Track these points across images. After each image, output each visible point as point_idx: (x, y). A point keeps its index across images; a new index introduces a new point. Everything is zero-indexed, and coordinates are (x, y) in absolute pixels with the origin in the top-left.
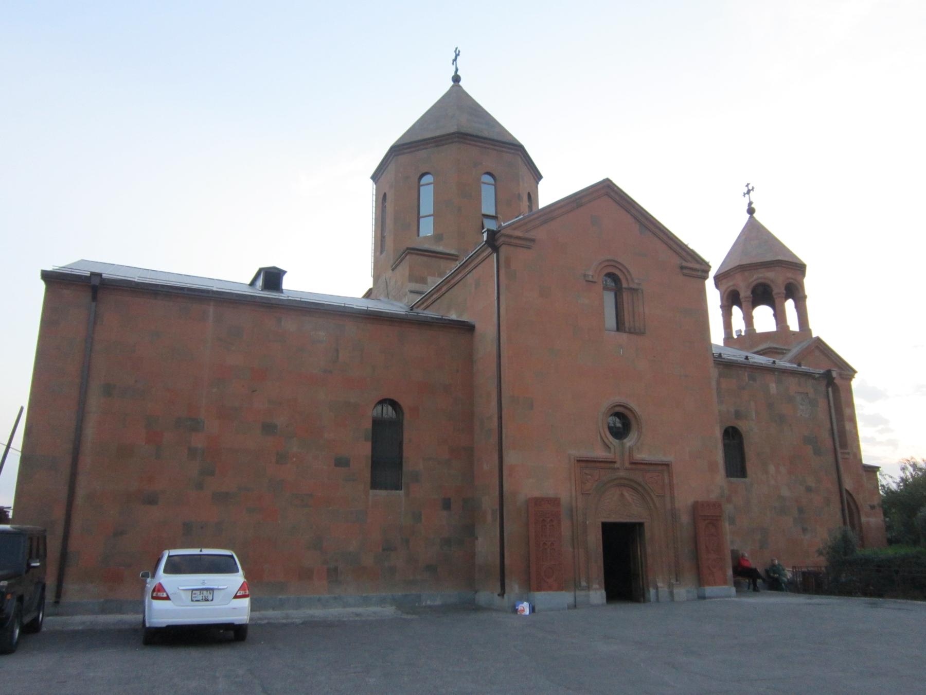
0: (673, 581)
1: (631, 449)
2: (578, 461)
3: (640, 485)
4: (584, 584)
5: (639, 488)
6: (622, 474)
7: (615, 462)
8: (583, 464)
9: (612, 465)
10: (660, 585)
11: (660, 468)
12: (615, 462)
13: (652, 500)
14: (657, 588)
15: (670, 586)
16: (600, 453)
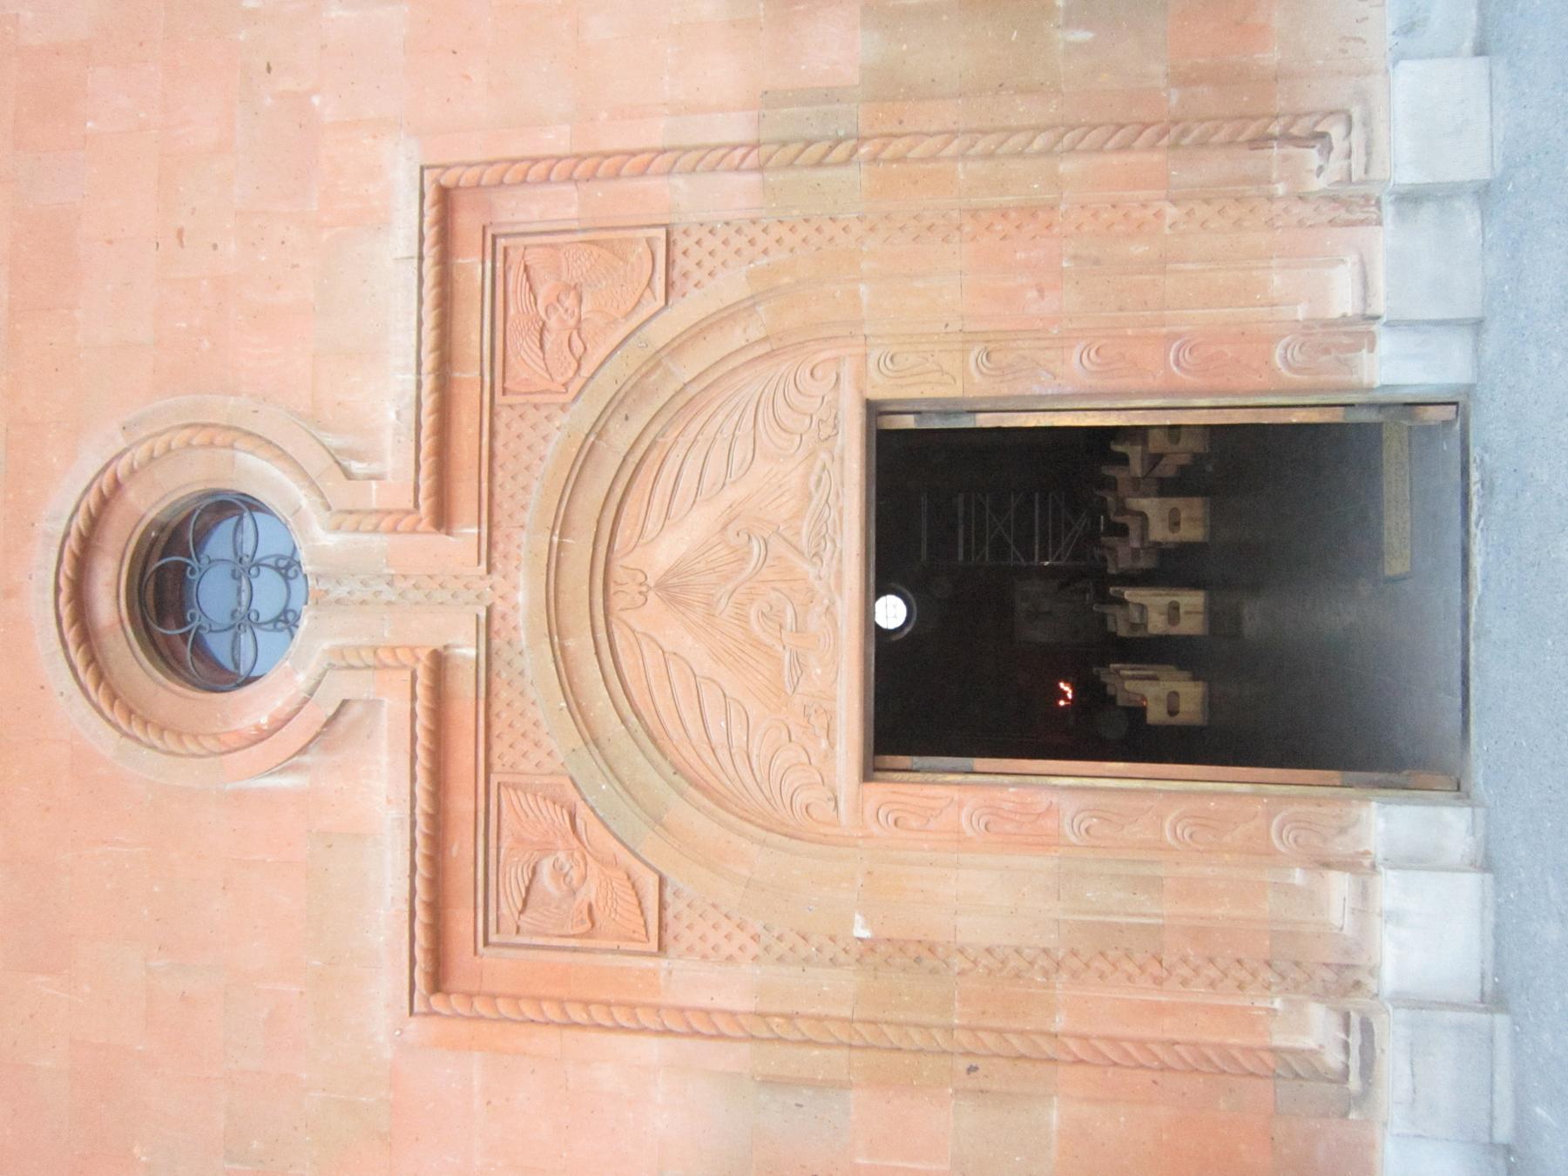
0: (1319, 172)
1: (348, 517)
2: (437, 982)
3: (599, 430)
4: (1315, 1030)
5: (621, 436)
6: (521, 594)
7: (439, 663)
8: (462, 923)
9: (464, 686)
10: (1343, 300)
11: (471, 265)
12: (439, 663)
13: (699, 331)
14: (1360, 329)
15: (1352, 204)
16: (378, 788)
